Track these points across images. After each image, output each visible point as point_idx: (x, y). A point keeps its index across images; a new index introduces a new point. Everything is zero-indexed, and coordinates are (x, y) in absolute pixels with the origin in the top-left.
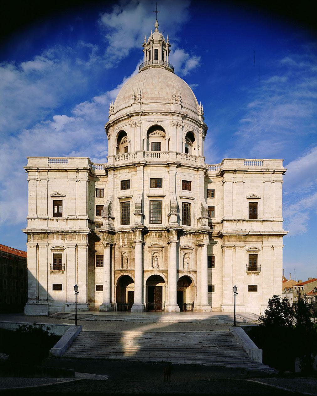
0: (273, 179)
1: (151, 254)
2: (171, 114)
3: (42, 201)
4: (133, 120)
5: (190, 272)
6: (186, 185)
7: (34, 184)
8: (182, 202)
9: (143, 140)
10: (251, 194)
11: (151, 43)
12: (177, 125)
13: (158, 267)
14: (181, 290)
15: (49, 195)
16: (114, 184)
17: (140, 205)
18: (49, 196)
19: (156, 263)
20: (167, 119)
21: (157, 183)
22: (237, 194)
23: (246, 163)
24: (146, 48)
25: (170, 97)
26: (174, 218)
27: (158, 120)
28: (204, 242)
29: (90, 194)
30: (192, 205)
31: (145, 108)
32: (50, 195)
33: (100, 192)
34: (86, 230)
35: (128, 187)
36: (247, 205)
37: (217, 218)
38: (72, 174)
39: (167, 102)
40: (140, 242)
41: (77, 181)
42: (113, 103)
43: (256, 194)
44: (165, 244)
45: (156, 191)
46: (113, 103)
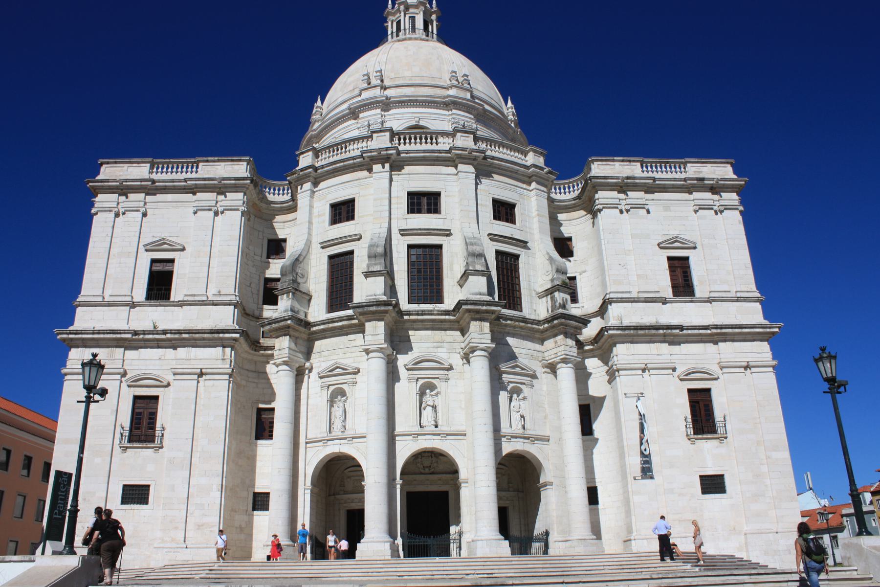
0: (717, 203)
1: (415, 388)
4: (364, 118)
6: (504, 211)
8: (498, 253)
15: (141, 246)
16: (311, 213)
17: (380, 250)
18: (142, 249)
22: (633, 236)
24: (391, 18)
25: (447, 77)
26: (477, 287)
29: (251, 247)
32: (145, 246)
33: (276, 247)
35: (350, 216)
36: (665, 264)
37: (585, 305)
40: (381, 350)
41: (216, 214)
42: (322, 102)
44: (456, 360)
46: (322, 102)
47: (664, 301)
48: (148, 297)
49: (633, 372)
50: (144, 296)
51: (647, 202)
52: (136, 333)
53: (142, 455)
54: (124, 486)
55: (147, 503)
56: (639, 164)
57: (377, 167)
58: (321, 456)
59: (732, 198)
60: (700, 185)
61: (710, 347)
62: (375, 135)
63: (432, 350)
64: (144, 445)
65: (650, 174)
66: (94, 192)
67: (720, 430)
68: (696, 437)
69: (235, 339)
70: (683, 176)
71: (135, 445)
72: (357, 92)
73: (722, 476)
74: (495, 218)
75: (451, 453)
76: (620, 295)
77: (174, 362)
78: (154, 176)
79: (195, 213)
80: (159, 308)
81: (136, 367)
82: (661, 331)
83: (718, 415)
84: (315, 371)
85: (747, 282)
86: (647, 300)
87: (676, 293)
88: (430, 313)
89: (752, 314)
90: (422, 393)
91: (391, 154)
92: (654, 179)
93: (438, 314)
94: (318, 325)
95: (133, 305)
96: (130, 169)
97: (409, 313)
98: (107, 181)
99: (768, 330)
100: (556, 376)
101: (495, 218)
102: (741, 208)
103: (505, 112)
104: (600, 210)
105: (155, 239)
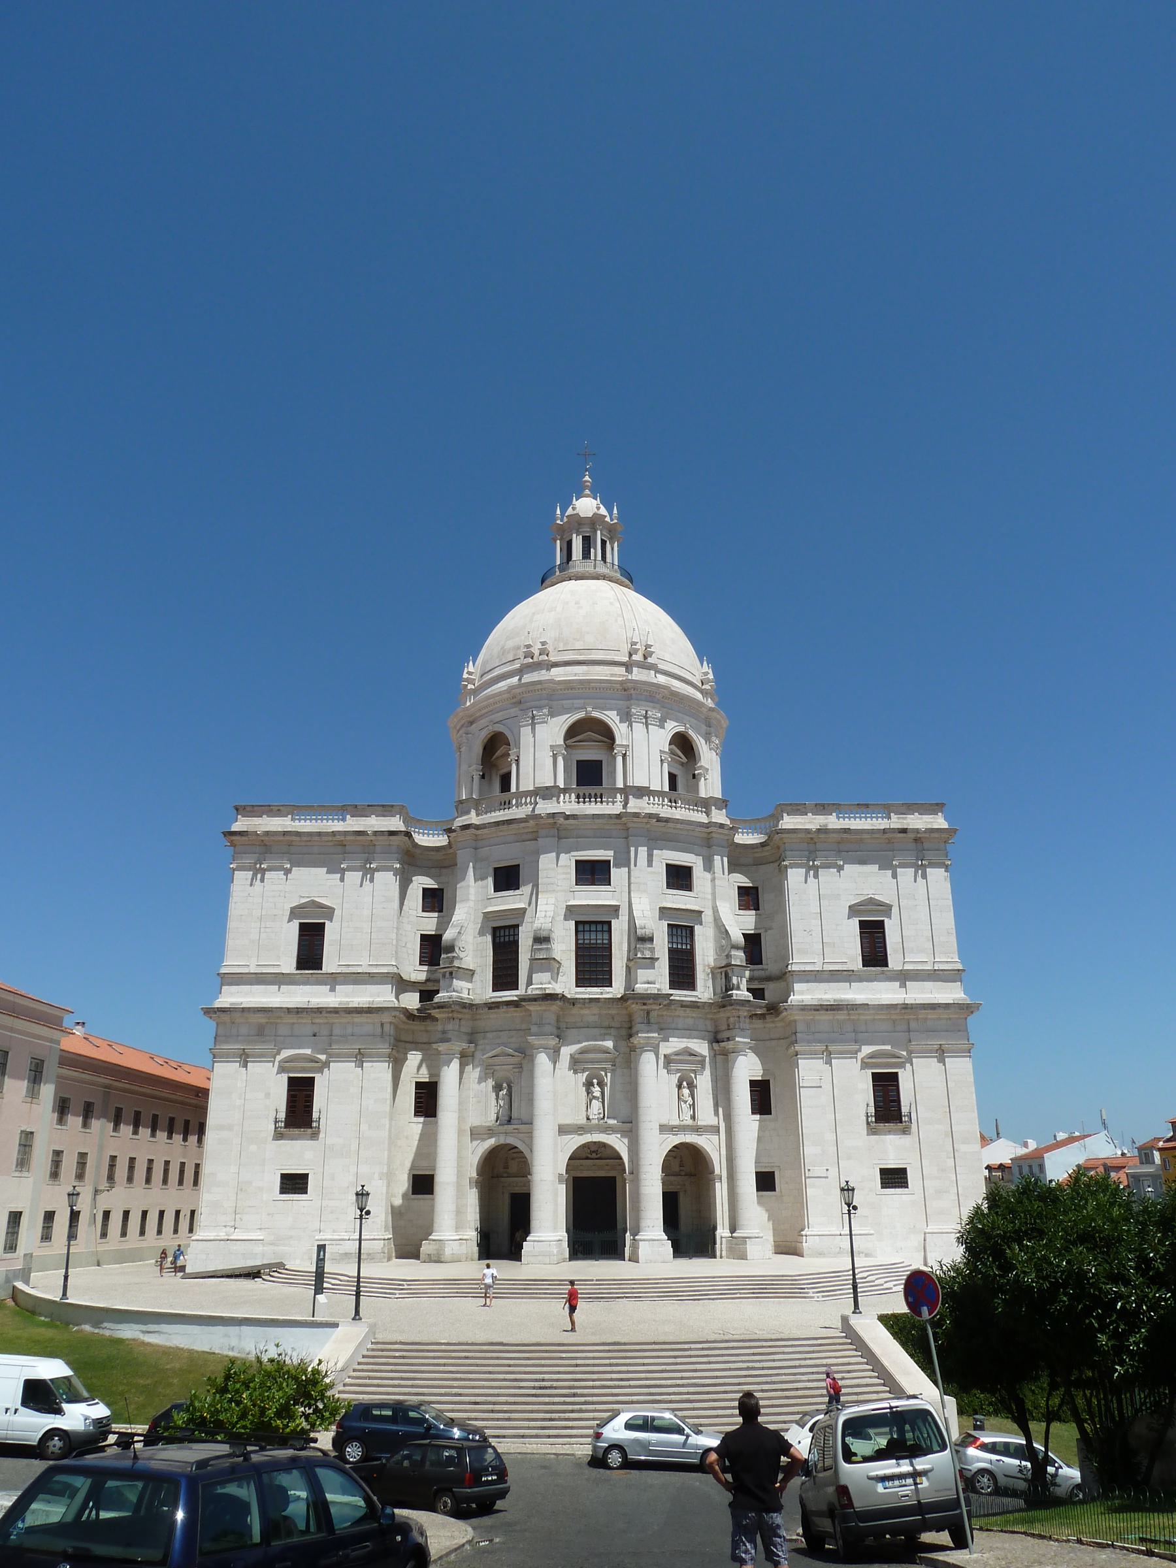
1: (583, 1077)
5: (697, 1129)
6: (679, 877)
9: (555, 757)
12: (646, 717)
14: (671, 1189)
25: (625, 649)
39: (617, 659)
43: (876, 897)
45: (593, 896)
48: (298, 968)
50: (294, 965)
54: (284, 1176)
55: (306, 1193)
73: (905, 1169)
74: (669, 886)
75: (617, 1148)
84: (478, 1055)
90: (589, 1085)
97: (573, 1002)
100: (726, 1062)
101: (669, 886)
104: (786, 867)
105: (303, 901)
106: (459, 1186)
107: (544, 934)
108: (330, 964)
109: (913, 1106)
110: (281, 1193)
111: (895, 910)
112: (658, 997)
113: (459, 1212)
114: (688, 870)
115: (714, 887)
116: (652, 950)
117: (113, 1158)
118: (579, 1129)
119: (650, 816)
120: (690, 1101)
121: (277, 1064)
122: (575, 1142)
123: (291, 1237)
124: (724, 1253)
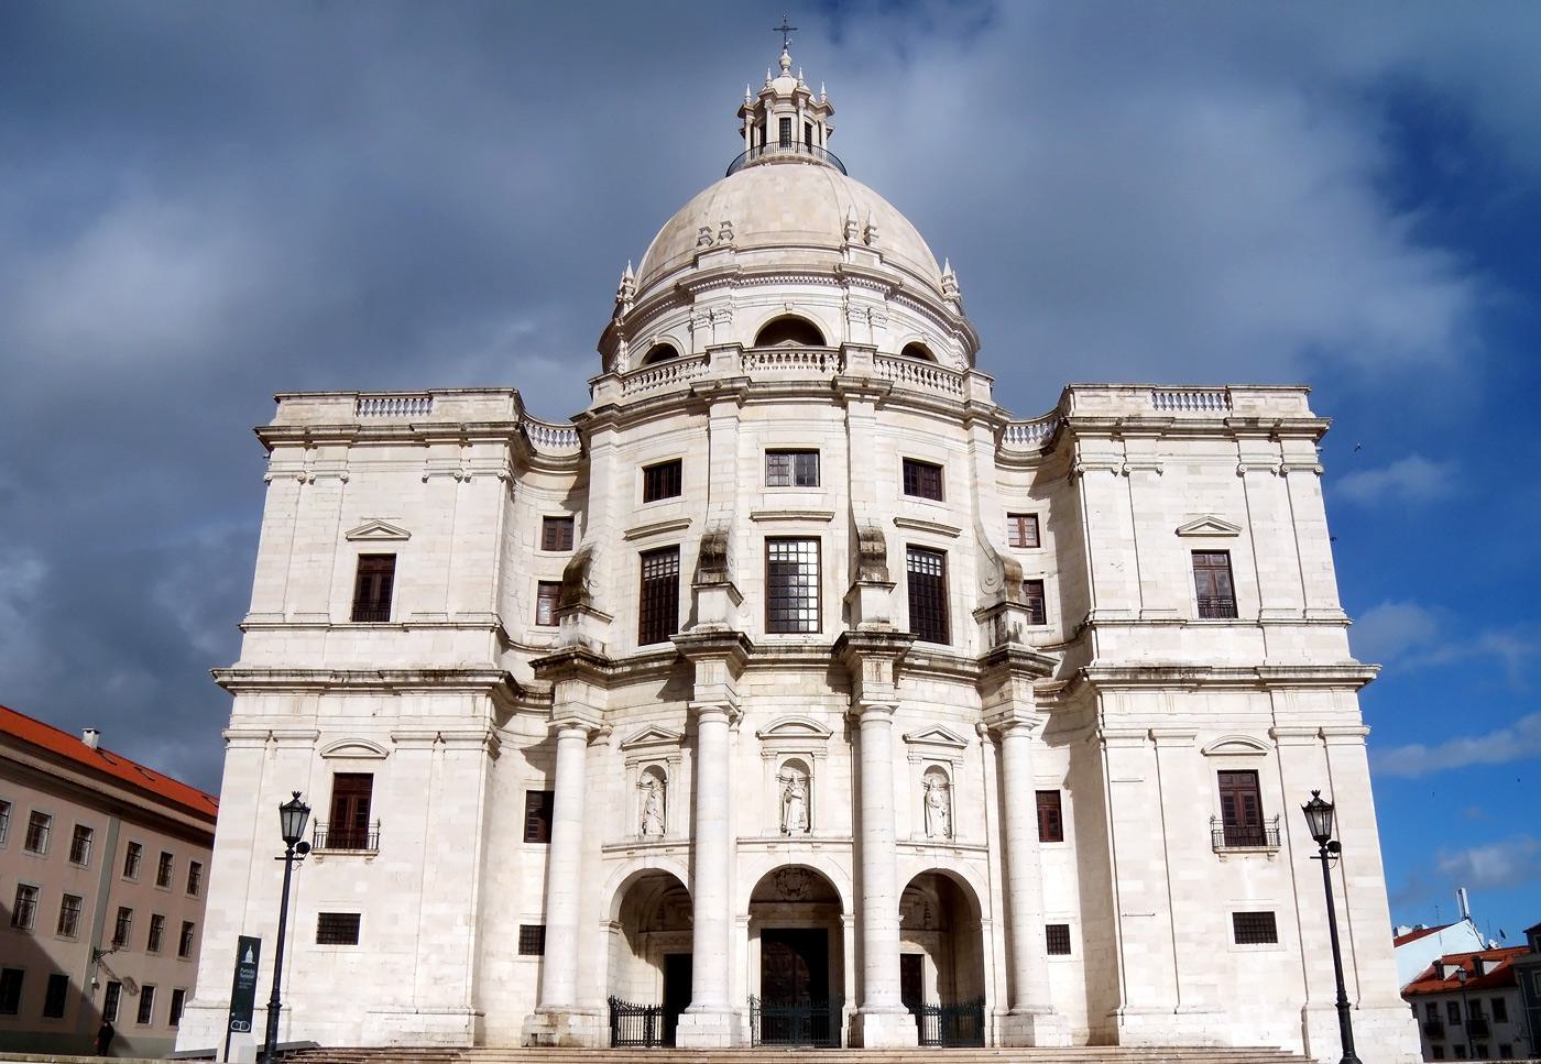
2: (841, 277)
3: (314, 556)
4: (702, 302)
6: (922, 478)
7: (286, 495)
10: (1195, 518)
11: (768, 102)
13: (808, 831)
19: (797, 807)
20: (827, 296)
21: (800, 464)
23: (1159, 403)
25: (840, 232)
27: (794, 298)
28: (1016, 712)
30: (952, 558)
31: (746, 261)
34: (481, 673)
35: (674, 488)
38: (443, 452)
43: (1215, 516)
47: (1182, 624)
49: (1129, 742)
50: (349, 613)
51: (1160, 459)
52: (335, 674)
53: (348, 864)
56: (1149, 394)
57: (715, 410)
58: (627, 873)
59: (1304, 450)
60: (1252, 426)
61: (1260, 699)
62: (713, 356)
63: (800, 708)
64: (352, 851)
65: (1168, 413)
66: (267, 443)
67: (1271, 838)
68: (1228, 849)
69: (494, 685)
70: (1224, 414)
71: (336, 851)
72: (689, 258)
74: (908, 491)
76: (1110, 616)
77: (395, 721)
78: (363, 420)
79: (425, 480)
80: (374, 634)
81: (337, 729)
82: (1177, 676)
83: (1269, 813)
84: (615, 740)
85: (1325, 594)
86: (1154, 624)
87: (1202, 614)
88: (799, 649)
89: (1332, 647)
91: (740, 389)
92: (1173, 420)
93: (811, 652)
94: (621, 666)
95: (330, 628)
96: (324, 408)
98: (288, 428)
99: (1356, 675)
101: (908, 491)
102: (1320, 469)
103: (938, 284)
104: (1081, 474)
105: (365, 523)
106: (578, 932)
107: (718, 549)
108: (398, 613)
109: (1282, 819)
110: (320, 940)
111: (1245, 535)
112: (895, 636)
113: (579, 973)
114: (936, 469)
115: (975, 497)
116: (886, 572)
117: (124, 912)
118: (771, 844)
119: (881, 382)
120: (943, 807)
121: (316, 754)
122: (762, 864)
123: (332, 1007)
124: (997, 1039)
